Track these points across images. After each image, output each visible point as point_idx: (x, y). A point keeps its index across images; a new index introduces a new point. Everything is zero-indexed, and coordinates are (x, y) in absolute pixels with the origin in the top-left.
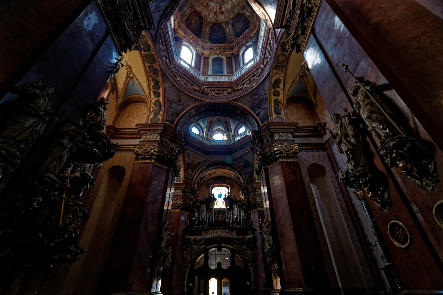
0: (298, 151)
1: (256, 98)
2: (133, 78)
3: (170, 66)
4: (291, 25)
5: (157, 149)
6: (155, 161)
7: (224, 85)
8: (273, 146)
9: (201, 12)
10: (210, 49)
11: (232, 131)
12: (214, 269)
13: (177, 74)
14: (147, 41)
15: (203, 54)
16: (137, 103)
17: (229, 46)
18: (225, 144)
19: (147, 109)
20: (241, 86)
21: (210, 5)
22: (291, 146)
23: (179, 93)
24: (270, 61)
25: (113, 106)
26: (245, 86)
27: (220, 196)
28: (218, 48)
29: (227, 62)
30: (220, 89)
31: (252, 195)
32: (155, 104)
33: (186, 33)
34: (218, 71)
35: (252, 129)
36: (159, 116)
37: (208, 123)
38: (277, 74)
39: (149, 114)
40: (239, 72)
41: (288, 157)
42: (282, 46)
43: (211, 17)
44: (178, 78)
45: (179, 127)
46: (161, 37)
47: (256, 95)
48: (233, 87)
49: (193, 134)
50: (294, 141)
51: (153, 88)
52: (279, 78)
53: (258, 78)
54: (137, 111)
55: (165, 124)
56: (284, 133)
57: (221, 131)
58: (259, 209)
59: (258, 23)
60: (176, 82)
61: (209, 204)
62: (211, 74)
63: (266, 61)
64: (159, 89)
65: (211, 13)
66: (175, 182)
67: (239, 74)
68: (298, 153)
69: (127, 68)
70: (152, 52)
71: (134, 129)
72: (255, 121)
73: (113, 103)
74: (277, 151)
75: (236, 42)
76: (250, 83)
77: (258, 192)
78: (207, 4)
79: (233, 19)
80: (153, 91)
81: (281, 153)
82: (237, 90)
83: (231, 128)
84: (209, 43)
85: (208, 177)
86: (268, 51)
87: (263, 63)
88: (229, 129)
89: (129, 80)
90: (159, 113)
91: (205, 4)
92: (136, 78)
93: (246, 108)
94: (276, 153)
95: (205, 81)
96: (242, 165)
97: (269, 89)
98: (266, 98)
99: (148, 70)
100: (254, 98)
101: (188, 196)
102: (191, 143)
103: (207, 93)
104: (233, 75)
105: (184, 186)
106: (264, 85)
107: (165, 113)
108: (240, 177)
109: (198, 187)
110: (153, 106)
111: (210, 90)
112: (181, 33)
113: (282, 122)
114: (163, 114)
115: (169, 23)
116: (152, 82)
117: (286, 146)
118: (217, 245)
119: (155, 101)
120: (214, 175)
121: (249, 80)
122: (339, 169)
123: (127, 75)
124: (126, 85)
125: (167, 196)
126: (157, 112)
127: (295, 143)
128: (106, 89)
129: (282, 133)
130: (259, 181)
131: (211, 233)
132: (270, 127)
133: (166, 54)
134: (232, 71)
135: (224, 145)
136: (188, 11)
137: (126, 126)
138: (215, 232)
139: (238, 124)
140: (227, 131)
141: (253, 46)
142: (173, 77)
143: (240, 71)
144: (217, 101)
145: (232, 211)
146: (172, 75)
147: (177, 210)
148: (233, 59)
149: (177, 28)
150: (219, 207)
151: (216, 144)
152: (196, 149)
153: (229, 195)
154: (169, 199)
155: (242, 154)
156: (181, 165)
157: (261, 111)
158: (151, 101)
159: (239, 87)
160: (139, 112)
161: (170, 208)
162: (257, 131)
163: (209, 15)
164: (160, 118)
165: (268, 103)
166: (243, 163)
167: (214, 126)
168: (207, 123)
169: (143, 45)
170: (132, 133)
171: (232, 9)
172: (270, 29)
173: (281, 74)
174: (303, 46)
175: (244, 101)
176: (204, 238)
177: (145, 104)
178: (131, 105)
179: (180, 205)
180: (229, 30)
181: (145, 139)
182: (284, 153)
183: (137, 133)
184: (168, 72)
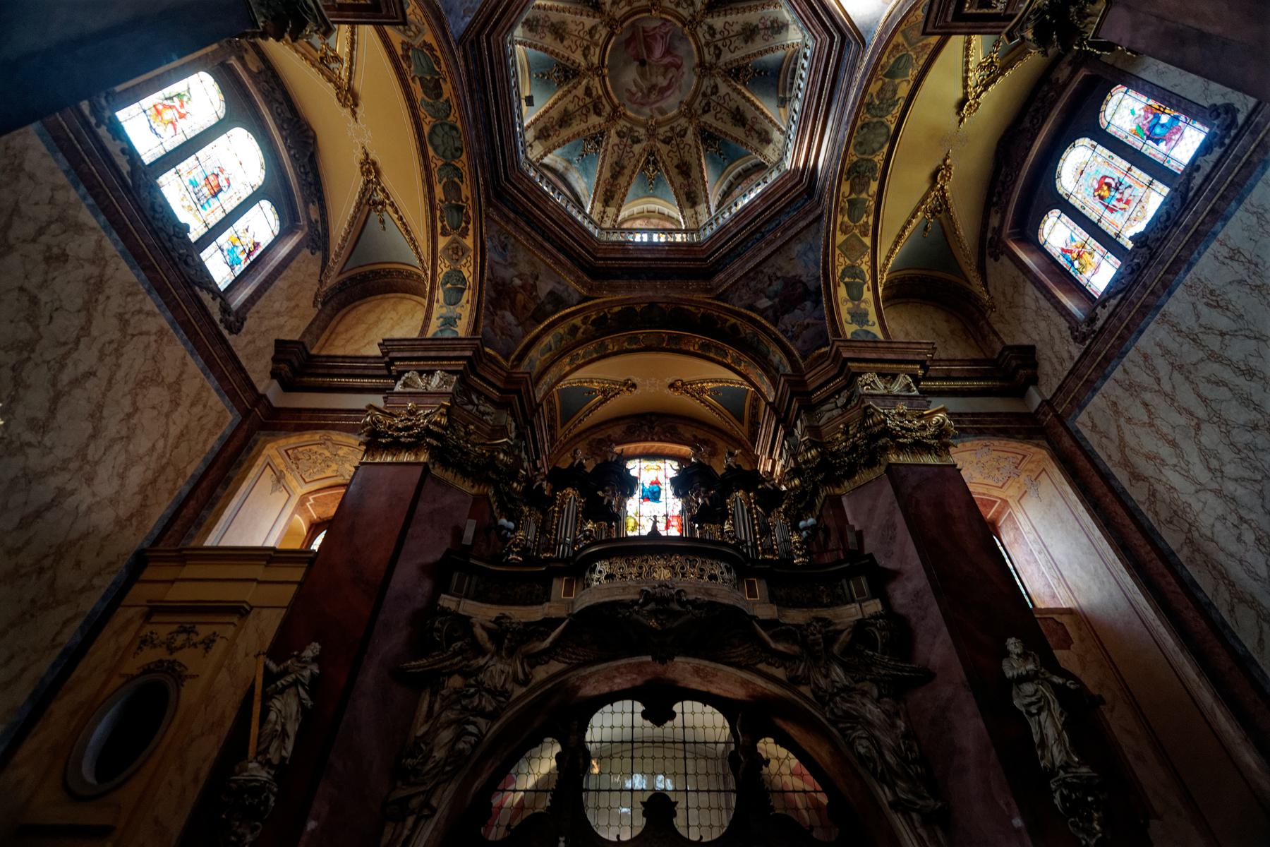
12: (619, 842)
57: (660, 219)
61: (600, 493)
88: (696, 196)
96: (766, 309)
101: (488, 418)
102: (521, 205)
120: (622, 402)
131: (610, 577)
138: (635, 570)
152: (548, 240)
156: (466, 274)
166: (770, 298)
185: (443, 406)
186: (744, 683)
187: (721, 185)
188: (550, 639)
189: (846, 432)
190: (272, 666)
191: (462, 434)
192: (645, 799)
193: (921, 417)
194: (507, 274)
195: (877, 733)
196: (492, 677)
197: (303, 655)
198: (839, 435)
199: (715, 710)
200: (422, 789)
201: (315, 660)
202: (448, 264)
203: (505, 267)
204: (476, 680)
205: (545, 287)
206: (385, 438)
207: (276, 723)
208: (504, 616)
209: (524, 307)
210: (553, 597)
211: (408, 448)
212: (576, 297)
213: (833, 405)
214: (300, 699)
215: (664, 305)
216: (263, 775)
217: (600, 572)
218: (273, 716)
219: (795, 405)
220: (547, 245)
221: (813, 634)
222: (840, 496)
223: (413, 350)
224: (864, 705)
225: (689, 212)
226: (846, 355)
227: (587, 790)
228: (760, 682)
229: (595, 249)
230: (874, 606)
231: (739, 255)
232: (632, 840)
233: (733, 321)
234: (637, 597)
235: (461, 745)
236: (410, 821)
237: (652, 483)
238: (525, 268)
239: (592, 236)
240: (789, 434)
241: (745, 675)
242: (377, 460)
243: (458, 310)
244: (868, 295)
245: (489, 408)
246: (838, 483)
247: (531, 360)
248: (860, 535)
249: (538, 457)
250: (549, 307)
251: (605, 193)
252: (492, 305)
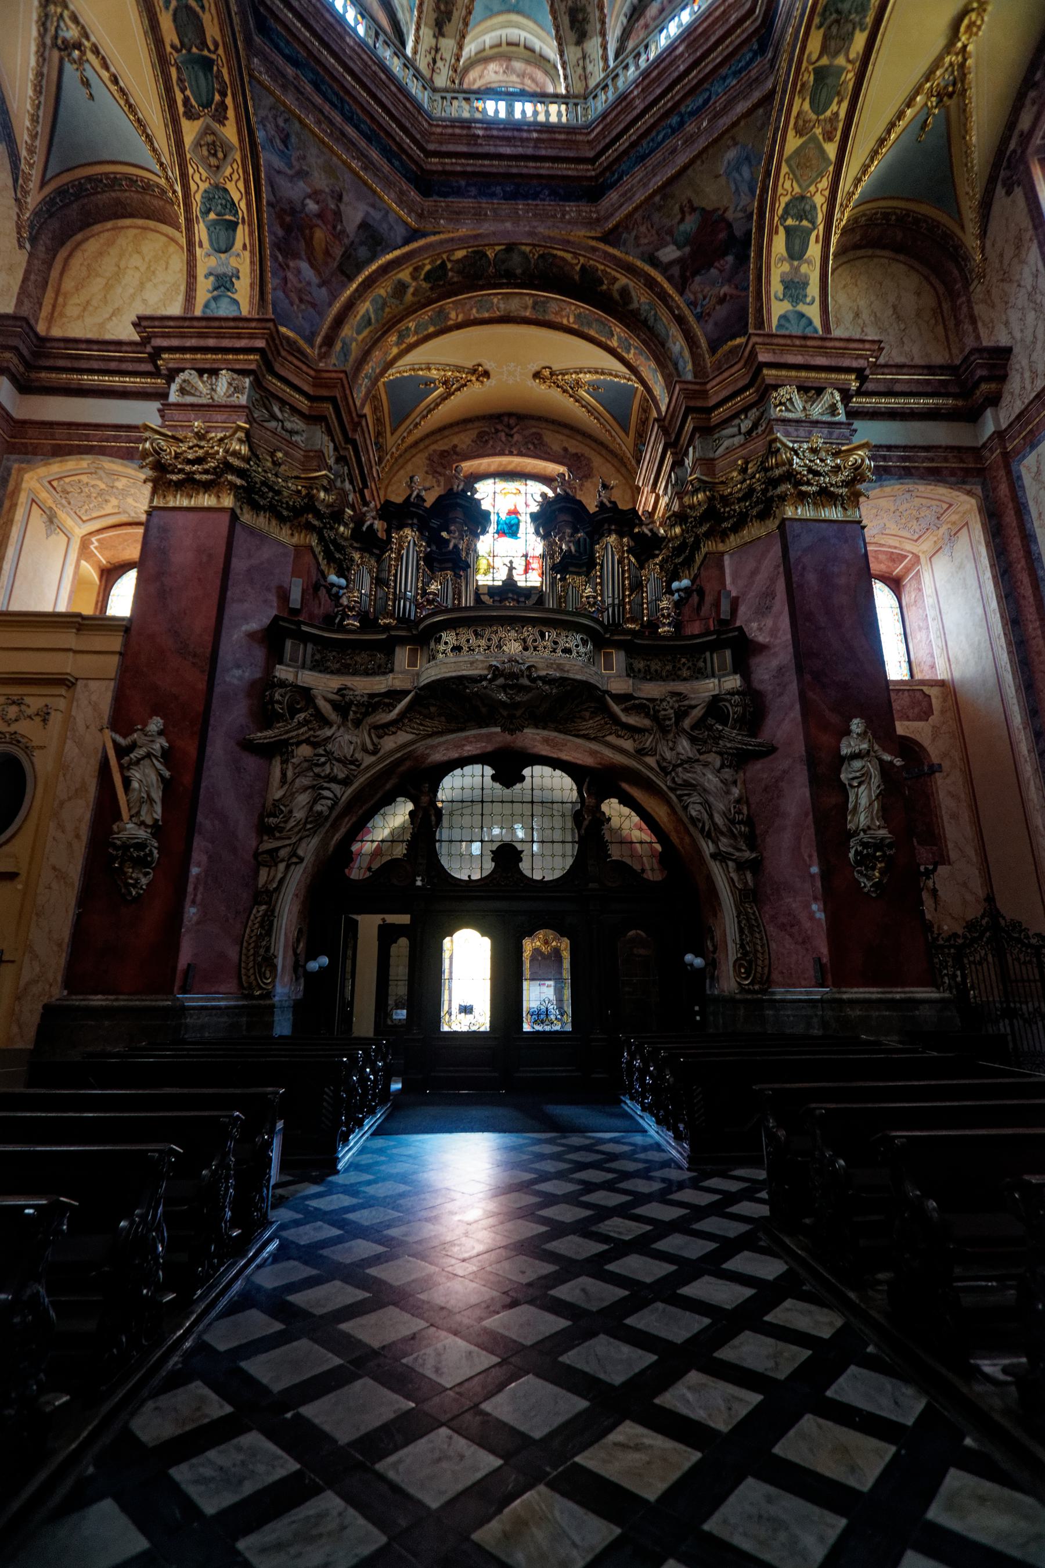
12: (470, 881)
57: (528, 62)
61: (444, 534)
88: (586, 20)
96: (671, 263)
101: (296, 438)
118: (494, 736)
131: (457, 649)
138: (483, 642)
140: (570, 36)
152: (349, 119)
156: (236, 196)
166: (679, 248)
176: (407, 685)
179: (230, 459)
185: (240, 428)
186: (593, 753)
188: (397, 711)
189: (744, 470)
190: (119, 739)
191: (269, 464)
192: (494, 849)
193: (836, 454)
194: (294, 191)
195: (711, 799)
196: (340, 746)
197: (148, 729)
198: (735, 474)
199: (564, 774)
200: (287, 842)
201: (161, 733)
202: (204, 175)
203: (291, 179)
204: (325, 750)
205: (354, 214)
206: (173, 472)
207: (140, 791)
208: (346, 688)
209: (327, 253)
210: (396, 668)
211: (206, 487)
212: (401, 232)
213: (736, 429)
214: (157, 770)
215: (528, 249)
216: (142, 834)
217: (446, 643)
218: (135, 785)
219: (689, 426)
220: (350, 130)
221: (665, 710)
222: (722, 554)
223: (182, 336)
224: (704, 774)
225: (573, 53)
226: (763, 357)
227: (440, 841)
228: (608, 753)
229: (423, 133)
230: (733, 682)
231: (642, 158)
232: (481, 879)
233: (623, 281)
234: (486, 672)
235: (318, 808)
236: (282, 867)
238: (321, 181)
239: (419, 107)
240: (678, 463)
241: (594, 746)
242: (171, 504)
243: (233, 262)
244: (814, 250)
245: (295, 423)
246: (724, 536)
247: (344, 343)
248: (735, 604)
249: (365, 486)
250: (363, 252)
252: (280, 250)
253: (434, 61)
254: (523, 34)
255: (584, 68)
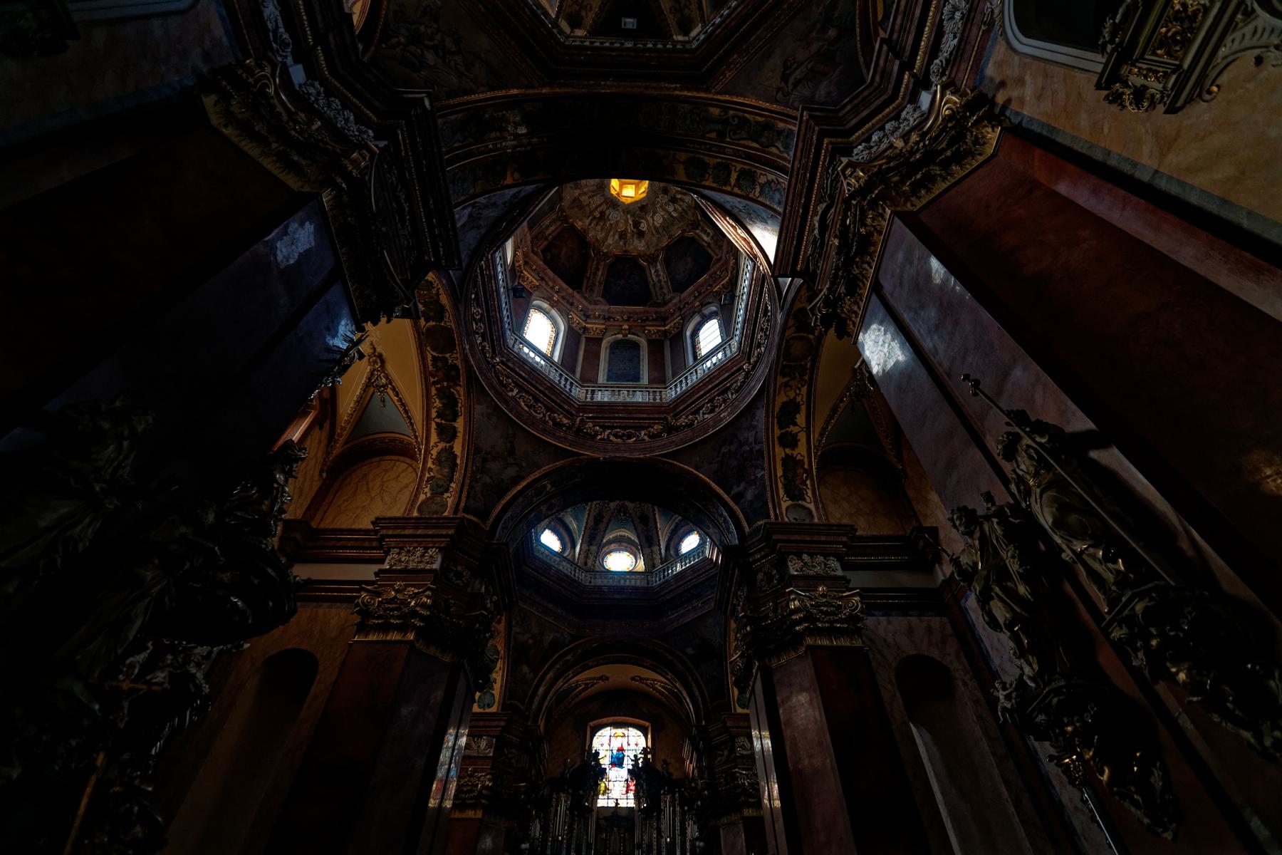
0: (862, 611)
1: (730, 451)
2: (384, 386)
3: (493, 358)
4: (819, 272)
5: (428, 597)
6: (416, 635)
7: (642, 412)
8: (784, 594)
9: (585, 231)
10: (605, 319)
11: (659, 545)
13: (510, 380)
14: (438, 294)
15: (585, 329)
16: (388, 457)
17: (656, 313)
18: (638, 584)
19: (414, 475)
20: (687, 417)
21: (610, 217)
22: (841, 598)
23: (511, 431)
24: (766, 355)
25: (316, 462)
26: (700, 417)
27: (618, 762)
28: (625, 317)
29: (649, 352)
30: (628, 424)
31: (724, 759)
32: (438, 461)
33: (542, 279)
34: (625, 375)
35: (721, 542)
36: (446, 495)
37: (591, 518)
38: (788, 389)
39: (417, 488)
40: (683, 378)
41: (831, 632)
42: (797, 317)
43: (612, 244)
44: (512, 391)
45: (503, 528)
46: (475, 285)
47: (731, 444)
48: (666, 419)
49: (542, 550)
50: (849, 581)
51: (437, 417)
52: (795, 398)
53: (734, 396)
54: (384, 480)
55: (462, 519)
56: (817, 554)
58: (748, 812)
59: (732, 262)
60: (506, 402)
62: (605, 382)
63: (756, 354)
64: (455, 420)
65: (611, 233)
66: (476, 709)
67: (684, 385)
68: (862, 619)
69: (371, 360)
70: (448, 324)
71: (367, 532)
72: (728, 518)
73: (316, 454)
74: (797, 610)
75: (675, 304)
76: (712, 411)
77: (743, 747)
78: (603, 214)
79: (668, 248)
80: (437, 423)
81: (809, 618)
82: (678, 429)
83: (658, 536)
84: (601, 303)
85: (581, 693)
86: (762, 329)
87: (749, 359)
89: (374, 392)
90: (449, 486)
91: (597, 214)
92: (394, 389)
93: (701, 479)
94: (794, 617)
95: (589, 400)
97: (767, 429)
98: (760, 452)
99: (431, 368)
100: (724, 450)
103: (590, 434)
104: (666, 388)
105: (503, 724)
106: (754, 416)
107: (466, 488)
108: (685, 694)
109: (546, 725)
110: (433, 467)
111: (601, 427)
112: (530, 278)
113: (807, 521)
114: (458, 490)
115: (501, 254)
116: (437, 401)
117: (823, 596)
119: (439, 453)
121: (711, 401)
122: (995, 676)
123: (370, 379)
124: (363, 406)
125: (445, 756)
126: (441, 483)
127: (850, 586)
128: (306, 414)
129: (811, 555)
130: (745, 711)
132: (774, 537)
133: (485, 328)
134: (665, 376)
135: (637, 588)
136: (552, 228)
137: (344, 522)
139: (677, 524)
141: (719, 312)
142: (498, 387)
143: (686, 378)
144: (619, 457)
145: (658, 819)
146: (495, 381)
147: (470, 814)
148: (667, 344)
149: (520, 266)
150: (611, 803)
151: (611, 583)
153: (649, 756)
154: (449, 769)
155: (693, 616)
157: (746, 489)
158: (427, 451)
159: (683, 421)
160: (387, 481)
161: (448, 804)
162: (735, 546)
163: (606, 238)
164: (450, 501)
165: (766, 465)
167: (606, 528)
168: (588, 519)
169: (425, 305)
170: (358, 544)
171: (666, 226)
172: (764, 276)
173: (800, 389)
174: (854, 324)
175: (698, 459)
177: (408, 460)
178: (367, 462)
180: (657, 274)
181: (395, 564)
182: (818, 620)
183: (374, 544)
184: (485, 375)
187: (671, 524)
237: (618, 750)
251: (590, 536)
253: (588, 554)
254: (626, 534)
255: (652, 556)
